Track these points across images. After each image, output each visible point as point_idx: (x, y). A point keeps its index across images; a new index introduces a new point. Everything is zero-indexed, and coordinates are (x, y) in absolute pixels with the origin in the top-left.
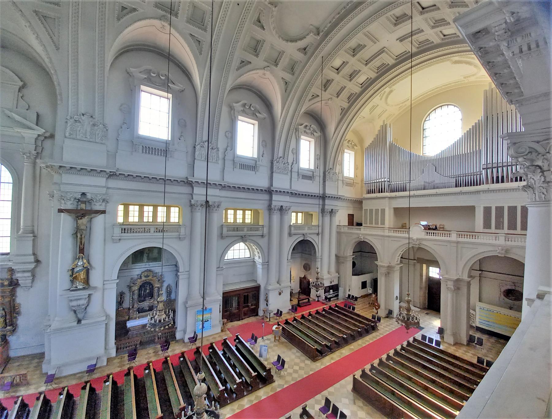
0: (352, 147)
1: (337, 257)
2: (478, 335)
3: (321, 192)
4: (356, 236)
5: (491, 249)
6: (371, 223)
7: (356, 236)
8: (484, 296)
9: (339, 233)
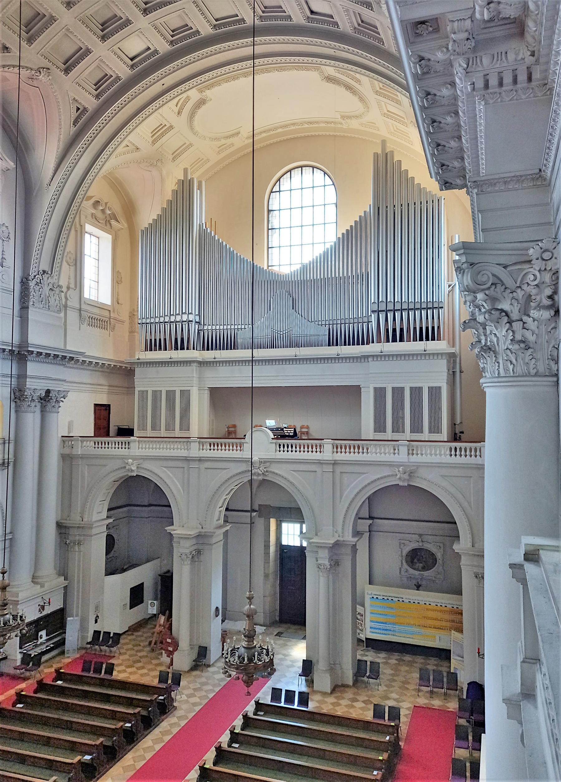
0: (106, 222)
2: (370, 656)
3: (16, 341)
4: (113, 465)
5: (386, 472)
8: (377, 571)
9: (67, 459)
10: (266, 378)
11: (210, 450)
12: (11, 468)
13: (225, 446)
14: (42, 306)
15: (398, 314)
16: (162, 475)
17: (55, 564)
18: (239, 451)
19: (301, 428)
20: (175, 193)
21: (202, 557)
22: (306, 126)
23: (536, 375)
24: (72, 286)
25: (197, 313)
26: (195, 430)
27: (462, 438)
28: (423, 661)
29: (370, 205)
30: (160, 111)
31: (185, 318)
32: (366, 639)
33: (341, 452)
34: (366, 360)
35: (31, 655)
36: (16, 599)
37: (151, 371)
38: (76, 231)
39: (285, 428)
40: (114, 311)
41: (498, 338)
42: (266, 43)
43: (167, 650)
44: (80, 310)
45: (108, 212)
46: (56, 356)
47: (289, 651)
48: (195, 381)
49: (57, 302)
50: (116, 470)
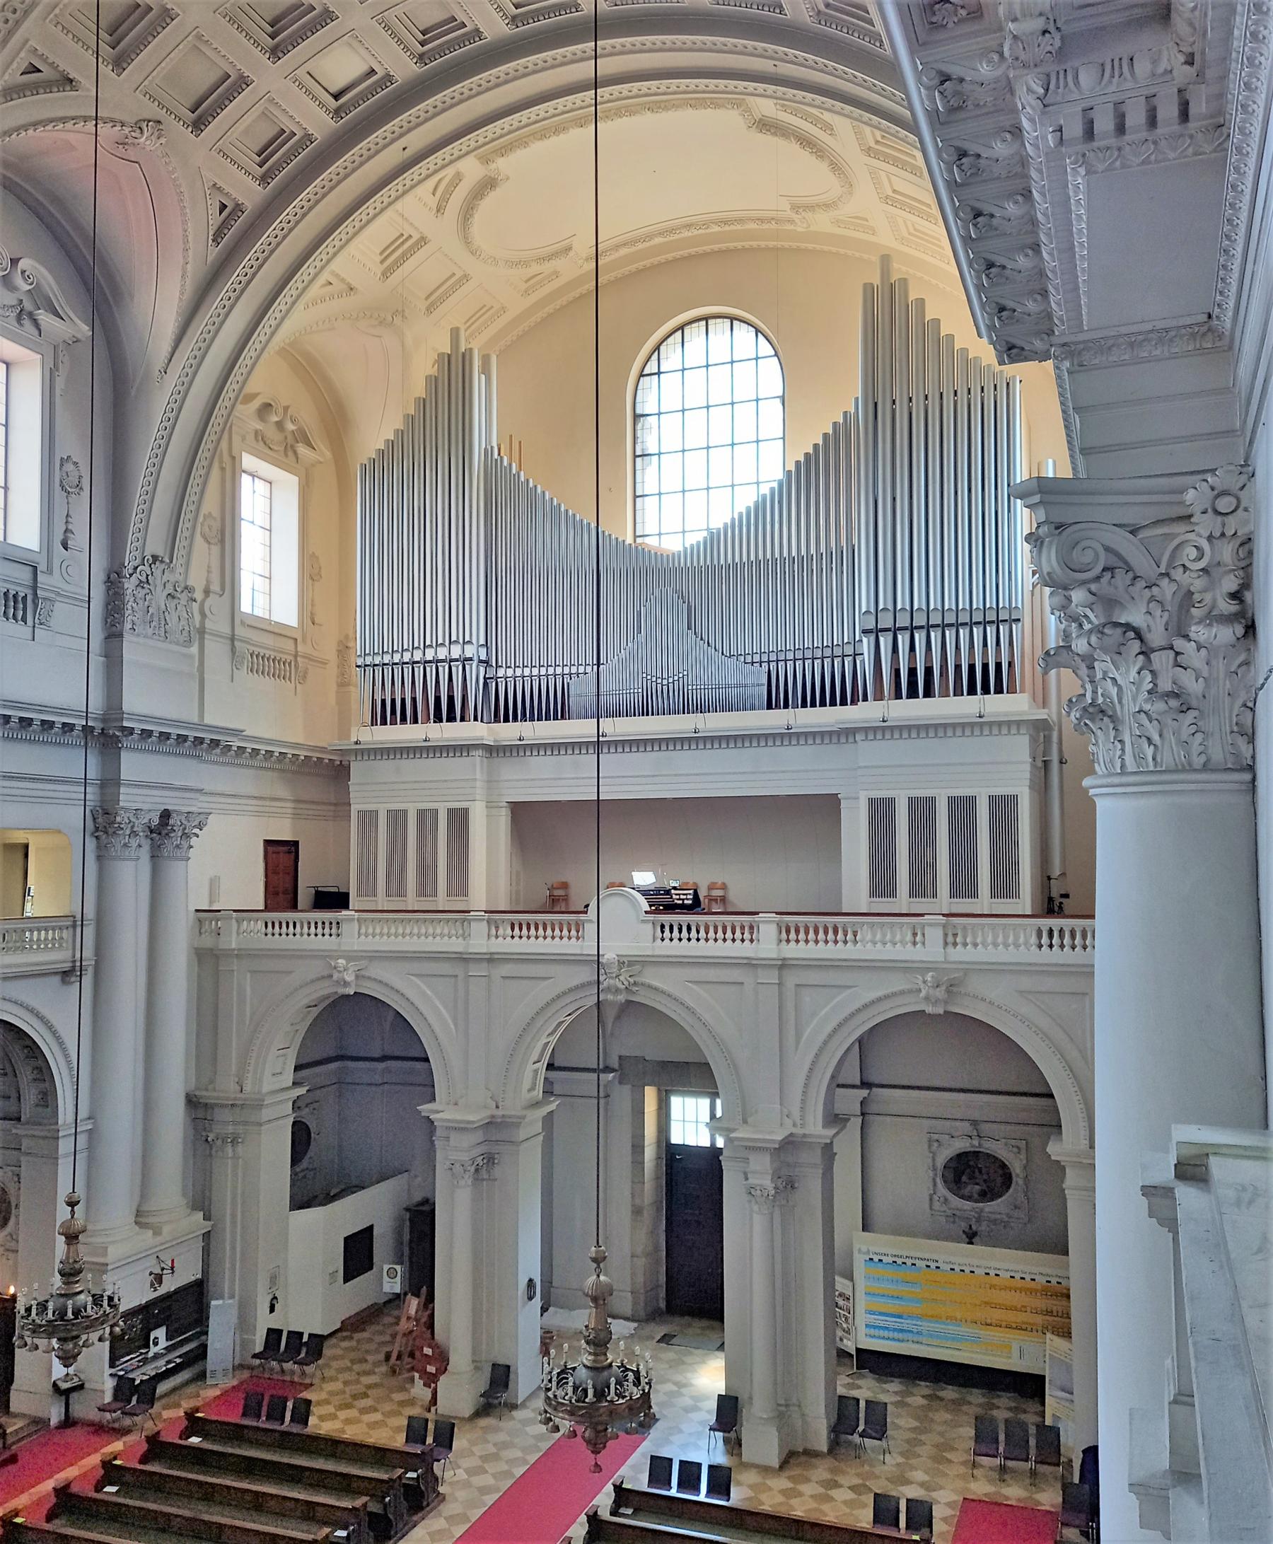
0: (286, 448)
1: (198, 1107)
2: (866, 1389)
3: (97, 704)
5: (898, 983)
6: (396, 886)
7: (317, 969)
9: (209, 960)
10: (628, 779)
11: (513, 937)
12: (88, 980)
13: (545, 929)
14: (150, 631)
15: (919, 637)
16: (410, 993)
17: (184, 1187)
18: (574, 940)
19: (710, 888)
20: (432, 382)
21: (497, 1171)
22: (716, 229)
23: (1206, 768)
24: (215, 587)
25: (482, 641)
26: (479, 897)
27: (1065, 907)
28: (981, 1400)
29: (857, 399)
30: (398, 205)
31: (456, 652)
32: (858, 1350)
33: (797, 941)
34: (851, 739)
35: (134, 1380)
36: (101, 1260)
37: (386, 768)
38: (223, 469)
39: (675, 888)
40: (304, 641)
41: (1120, 688)
42: (621, 53)
43: (424, 1373)
44: (232, 639)
45: (290, 427)
46: (182, 739)
47: (689, 1375)
48: (480, 790)
49: (183, 622)
50: (312, 981)
